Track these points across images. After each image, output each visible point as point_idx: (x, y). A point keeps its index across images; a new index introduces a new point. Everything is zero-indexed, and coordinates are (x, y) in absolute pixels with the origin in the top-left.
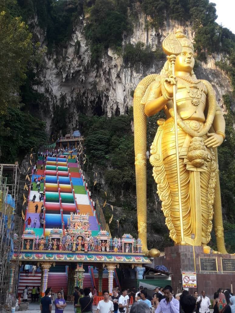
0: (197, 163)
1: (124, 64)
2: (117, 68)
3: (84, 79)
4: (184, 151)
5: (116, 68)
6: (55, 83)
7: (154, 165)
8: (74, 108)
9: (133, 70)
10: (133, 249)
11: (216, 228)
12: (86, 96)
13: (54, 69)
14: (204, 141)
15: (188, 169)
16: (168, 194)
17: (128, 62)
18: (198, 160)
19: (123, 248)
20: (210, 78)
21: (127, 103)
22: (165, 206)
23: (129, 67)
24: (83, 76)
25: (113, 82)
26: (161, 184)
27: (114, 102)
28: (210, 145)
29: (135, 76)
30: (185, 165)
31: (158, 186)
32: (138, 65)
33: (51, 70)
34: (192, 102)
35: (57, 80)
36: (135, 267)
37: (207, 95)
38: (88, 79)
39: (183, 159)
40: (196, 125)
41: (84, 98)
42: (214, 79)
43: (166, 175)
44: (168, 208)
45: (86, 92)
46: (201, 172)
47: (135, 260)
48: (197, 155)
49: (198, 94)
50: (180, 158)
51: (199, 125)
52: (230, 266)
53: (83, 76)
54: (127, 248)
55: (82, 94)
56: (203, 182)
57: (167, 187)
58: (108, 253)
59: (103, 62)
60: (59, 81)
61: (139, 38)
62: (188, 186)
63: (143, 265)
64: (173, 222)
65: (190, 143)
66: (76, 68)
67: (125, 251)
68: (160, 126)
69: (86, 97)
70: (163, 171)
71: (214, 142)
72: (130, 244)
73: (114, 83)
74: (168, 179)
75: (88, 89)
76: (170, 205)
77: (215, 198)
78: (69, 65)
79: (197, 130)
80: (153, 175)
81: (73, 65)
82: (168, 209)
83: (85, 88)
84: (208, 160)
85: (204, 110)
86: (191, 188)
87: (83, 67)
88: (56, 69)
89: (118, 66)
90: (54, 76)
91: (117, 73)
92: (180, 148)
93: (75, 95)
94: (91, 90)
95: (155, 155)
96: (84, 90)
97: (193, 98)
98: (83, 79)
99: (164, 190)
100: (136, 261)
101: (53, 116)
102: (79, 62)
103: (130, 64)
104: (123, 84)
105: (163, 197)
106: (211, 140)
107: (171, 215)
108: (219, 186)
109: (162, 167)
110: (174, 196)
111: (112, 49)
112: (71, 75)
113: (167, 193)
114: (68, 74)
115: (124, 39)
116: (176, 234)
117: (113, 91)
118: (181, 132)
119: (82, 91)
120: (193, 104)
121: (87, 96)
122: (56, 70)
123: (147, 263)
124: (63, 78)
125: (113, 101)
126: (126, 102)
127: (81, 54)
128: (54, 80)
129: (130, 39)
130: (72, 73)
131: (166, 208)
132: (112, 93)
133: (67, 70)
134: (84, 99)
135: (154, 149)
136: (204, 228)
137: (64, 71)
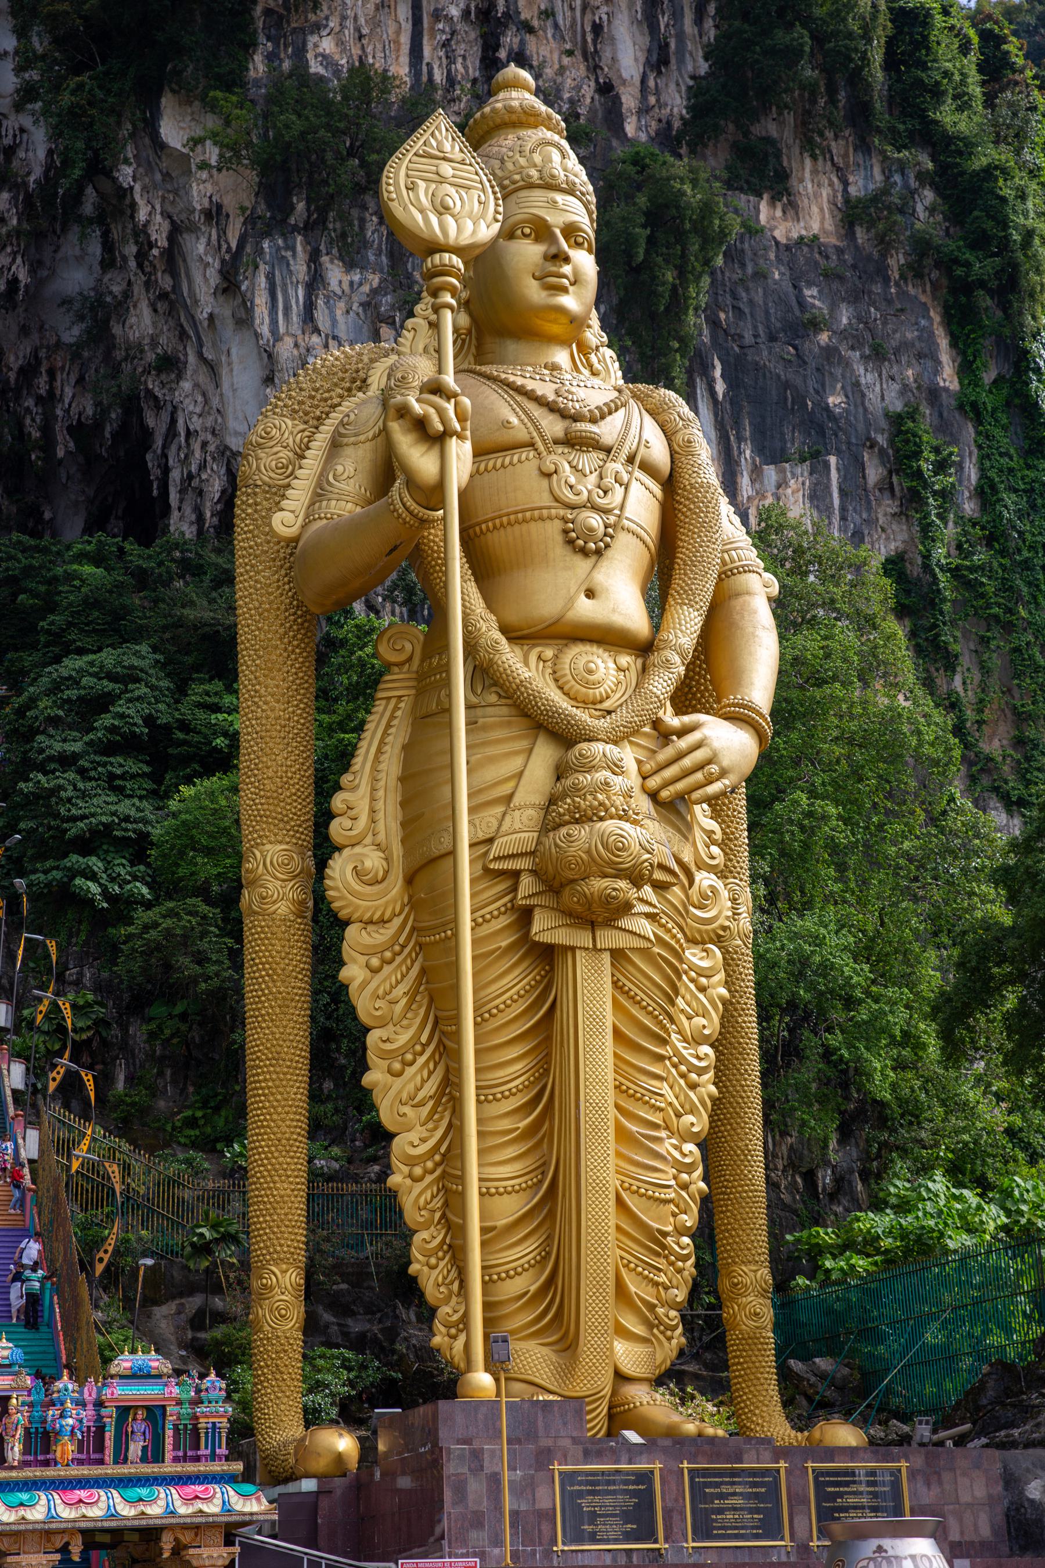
0: (588, 902)
1: (262, 209)
2: (222, 232)
3: (23, 276)
4: (517, 826)
5: (214, 232)
7: (353, 913)
9: (322, 247)
10: (169, 1441)
14: (639, 762)
15: (546, 938)
16: (431, 1087)
17: (289, 194)
18: (598, 885)
19: (107, 1435)
20: (813, 306)
22: (411, 1161)
23: (295, 229)
24: (14, 254)
25: (203, 315)
27: (212, 448)
29: (334, 286)
30: (525, 916)
31: (372, 1038)
32: (355, 213)
36: (178, 1549)
37: (672, 484)
39: (516, 874)
40: (590, 672)
41: (30, 402)
42: (833, 307)
43: (423, 971)
44: (432, 1172)
46: (618, 955)
47: (178, 1503)
48: (588, 852)
50: (487, 874)
52: (735, 1509)
53: (19, 260)
54: (139, 1436)
55: (12, 376)
56: (635, 1011)
57: (425, 1046)
58: (14, 1474)
59: (132, 188)
61: (365, 31)
62: (548, 1039)
63: (230, 1531)
64: (454, 1257)
65: (558, 779)
67: (121, 1458)
69: (39, 400)
70: (403, 947)
71: (700, 767)
72: (155, 1413)
73: (206, 323)
74: (431, 1000)
75: (53, 341)
76: (444, 1155)
77: (715, 1101)
79: (601, 702)
80: (344, 974)
82: (429, 1178)
83: (35, 336)
84: (658, 875)
85: (641, 574)
86: (562, 1045)
87: (15, 198)
89: (228, 216)
91: (223, 261)
92: (499, 810)
94: (75, 352)
95: (358, 849)
96: (25, 348)
98: (13, 283)
99: (411, 1064)
100: (183, 1510)
103: (301, 206)
104: (257, 336)
106: (681, 756)
107: (443, 1216)
109: (397, 922)
111: (187, 96)
113: (424, 1082)
115: (262, 39)
117: (203, 378)
119: (12, 358)
121: (51, 392)
123: (247, 1518)
125: (204, 444)
129: (304, 43)
131: (418, 1171)
132: (196, 385)
134: (28, 410)
135: (351, 813)
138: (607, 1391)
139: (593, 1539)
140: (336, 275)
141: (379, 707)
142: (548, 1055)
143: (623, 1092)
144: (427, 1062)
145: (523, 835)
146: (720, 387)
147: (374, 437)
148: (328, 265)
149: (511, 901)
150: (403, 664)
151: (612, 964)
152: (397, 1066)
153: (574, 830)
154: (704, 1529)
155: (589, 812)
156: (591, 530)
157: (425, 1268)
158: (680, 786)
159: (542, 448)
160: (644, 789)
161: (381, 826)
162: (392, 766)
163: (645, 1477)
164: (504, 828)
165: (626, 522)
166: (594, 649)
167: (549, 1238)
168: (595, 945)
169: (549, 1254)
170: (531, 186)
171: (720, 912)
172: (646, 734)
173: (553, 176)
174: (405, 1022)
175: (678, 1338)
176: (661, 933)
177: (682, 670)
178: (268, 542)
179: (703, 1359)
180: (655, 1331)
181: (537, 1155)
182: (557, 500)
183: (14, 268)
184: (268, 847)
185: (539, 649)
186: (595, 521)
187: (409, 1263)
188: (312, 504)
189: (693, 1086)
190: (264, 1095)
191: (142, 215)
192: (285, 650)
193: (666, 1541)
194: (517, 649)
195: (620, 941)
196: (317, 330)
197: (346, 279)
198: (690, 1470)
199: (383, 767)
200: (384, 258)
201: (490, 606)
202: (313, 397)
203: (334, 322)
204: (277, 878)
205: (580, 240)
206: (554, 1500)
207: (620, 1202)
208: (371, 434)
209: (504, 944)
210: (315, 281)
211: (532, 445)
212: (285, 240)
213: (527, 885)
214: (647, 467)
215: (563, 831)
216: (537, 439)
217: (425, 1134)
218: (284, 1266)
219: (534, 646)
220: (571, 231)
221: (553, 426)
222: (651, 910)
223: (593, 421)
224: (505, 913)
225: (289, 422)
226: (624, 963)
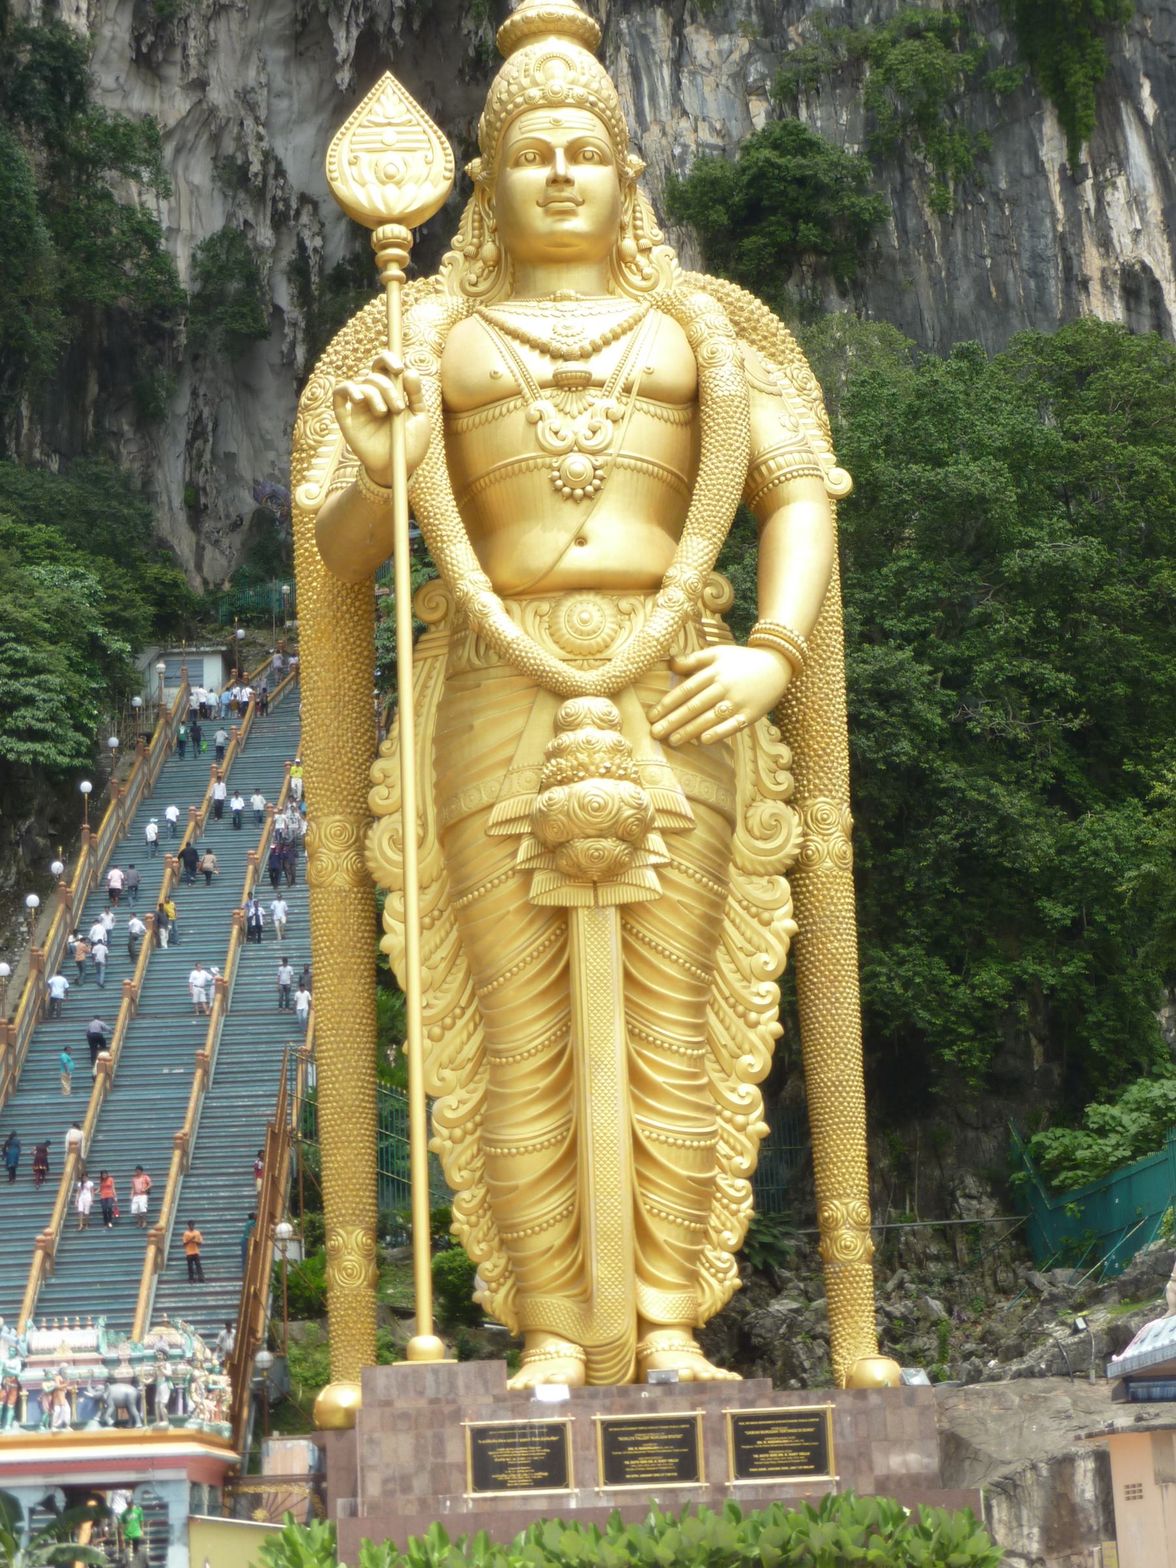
6: (296, 107)
9: (687, 17)
14: (648, 707)
16: (471, 1049)
28: (690, 728)
33: (244, 21)
34: (553, 480)
39: (519, 837)
40: (584, 622)
44: (472, 1133)
46: (625, 910)
49: (595, 422)
60: (322, 82)
68: (433, 628)
79: (600, 652)
82: (469, 1139)
90: (280, 53)
92: (502, 772)
112: (397, 26)
113: (463, 1044)
114: (371, 21)
120: (558, 490)
124: (339, 59)
128: (279, 82)
130: (401, 8)
135: (389, 781)
136: (661, 1233)
139: (503, 1485)
140: (702, 44)
144: (467, 1024)
146: (1150, 109)
148: (694, 36)
152: (437, 1031)
154: (615, 1473)
157: (466, 1227)
158: (690, 728)
159: (528, 395)
160: (654, 737)
163: (557, 1430)
168: (596, 902)
170: (535, 107)
171: (787, 840)
182: (543, 448)
183: (481, 32)
184: (323, 819)
185: (535, 604)
193: (577, 1486)
195: (627, 895)
196: (685, 113)
197: (714, 48)
198: (603, 1423)
200: (754, 18)
202: (355, 350)
203: (703, 100)
204: (330, 850)
205: (588, 155)
206: (465, 1453)
210: (680, 58)
211: (518, 393)
212: (644, 17)
216: (524, 385)
217: (467, 1096)
218: (350, 1228)
219: (532, 600)
221: (544, 368)
223: (585, 356)
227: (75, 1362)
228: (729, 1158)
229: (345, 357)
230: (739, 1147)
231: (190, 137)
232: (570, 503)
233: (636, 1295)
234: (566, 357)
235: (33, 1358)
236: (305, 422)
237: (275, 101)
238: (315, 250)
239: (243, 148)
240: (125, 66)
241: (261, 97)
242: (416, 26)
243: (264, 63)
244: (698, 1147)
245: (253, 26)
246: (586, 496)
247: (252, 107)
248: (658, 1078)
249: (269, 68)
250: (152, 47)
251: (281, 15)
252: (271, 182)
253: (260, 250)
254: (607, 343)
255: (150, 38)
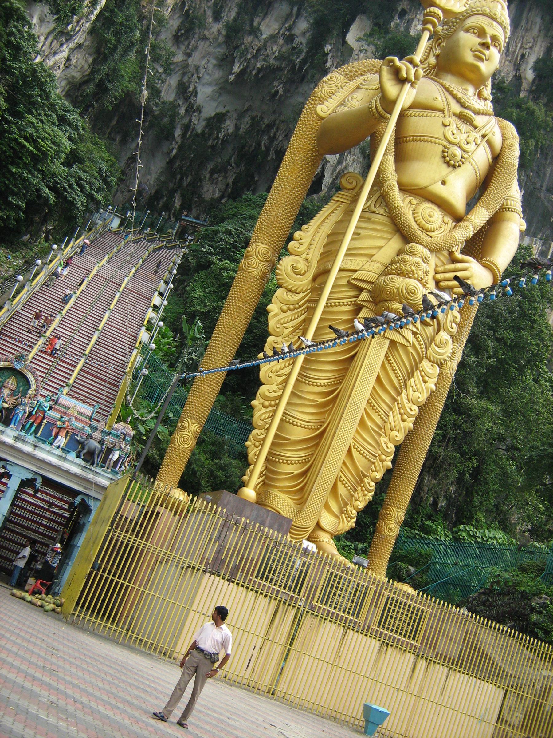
4: (370, 269)
7: (283, 283)
8: (234, 154)
11: (386, 509)
12: (272, 135)
13: (219, 45)
14: (436, 266)
21: (346, 168)
22: (265, 398)
26: (279, 339)
33: (210, 46)
35: (218, 74)
37: (497, 159)
38: (292, 96)
39: (361, 290)
40: (430, 216)
45: (275, 124)
46: (393, 343)
48: (398, 289)
49: (468, 140)
51: (440, 220)
55: (264, 126)
59: (327, 54)
62: (347, 369)
66: (272, 61)
70: (300, 307)
77: (410, 432)
78: (257, 48)
79: (430, 231)
80: (269, 307)
81: (268, 50)
88: (224, 46)
90: (214, 62)
92: (365, 259)
93: (246, 122)
95: (297, 257)
96: (273, 118)
97: (450, 143)
98: (277, 92)
101: (174, 152)
102: (284, 49)
105: (271, 375)
108: (440, 406)
109: (302, 295)
110: (302, 382)
112: (254, 73)
113: (285, 367)
114: (247, 67)
116: (263, 481)
118: (385, 219)
122: (222, 49)
126: (344, 164)
127: (296, 31)
131: (267, 403)
133: (249, 56)
135: (301, 241)
136: (342, 490)
137: (241, 58)
138: (311, 529)
141: (331, 203)
142: (344, 376)
143: (371, 406)
145: (371, 273)
147: (376, 89)
149: (355, 301)
150: (349, 190)
151: (389, 348)
153: (395, 277)
155: (405, 272)
156: (455, 155)
157: (253, 446)
160: (434, 278)
161: (311, 251)
162: (327, 228)
164: (364, 267)
165: (472, 161)
166: (436, 208)
167: (313, 454)
169: (309, 461)
170: (484, 14)
171: (446, 352)
172: (444, 255)
173: (495, 15)
174: (287, 338)
175: (352, 523)
176: (416, 344)
177: (471, 234)
178: (313, 121)
179: (360, 536)
180: (343, 515)
181: (322, 417)
182: (445, 137)
186: (458, 153)
187: (247, 440)
188: (337, 107)
189: (404, 421)
190: (216, 347)
191: (328, 65)
192: (302, 166)
194: (401, 194)
199: (322, 228)
201: (397, 170)
202: (356, 72)
205: (497, 44)
207: (349, 451)
208: (374, 87)
209: (344, 318)
213: (364, 296)
214: (489, 143)
215: (390, 276)
219: (410, 196)
220: (494, 38)
221: (456, 108)
222: (416, 331)
224: (350, 305)
225: (342, 77)
226: (394, 350)
227: (76, 418)
228: (373, 471)
229: (351, 72)
230: (378, 468)
231: (177, 69)
232: (445, 166)
233: (320, 513)
234: (466, 108)
235: (57, 407)
236: (323, 87)
237: (205, 75)
238: (194, 124)
239: (190, 82)
240: (170, 36)
241: (202, 70)
242: (260, 75)
243: (208, 61)
244: (369, 460)
245: (212, 49)
246: (454, 167)
247: (198, 73)
248: (369, 423)
249: (209, 64)
250: (182, 35)
251: (222, 51)
252: (192, 98)
253: (179, 114)
254: (483, 114)
255: (183, 32)
